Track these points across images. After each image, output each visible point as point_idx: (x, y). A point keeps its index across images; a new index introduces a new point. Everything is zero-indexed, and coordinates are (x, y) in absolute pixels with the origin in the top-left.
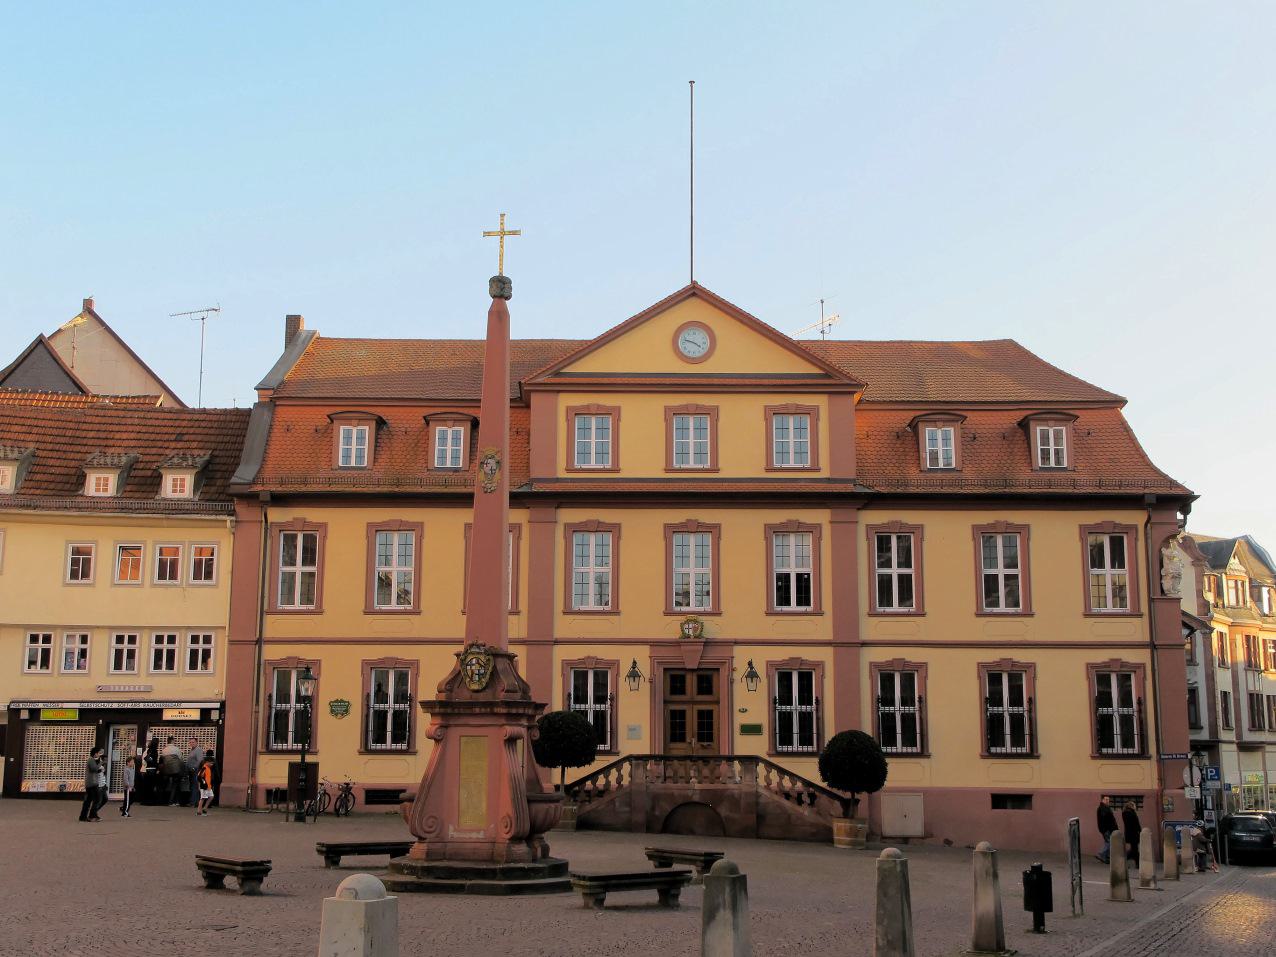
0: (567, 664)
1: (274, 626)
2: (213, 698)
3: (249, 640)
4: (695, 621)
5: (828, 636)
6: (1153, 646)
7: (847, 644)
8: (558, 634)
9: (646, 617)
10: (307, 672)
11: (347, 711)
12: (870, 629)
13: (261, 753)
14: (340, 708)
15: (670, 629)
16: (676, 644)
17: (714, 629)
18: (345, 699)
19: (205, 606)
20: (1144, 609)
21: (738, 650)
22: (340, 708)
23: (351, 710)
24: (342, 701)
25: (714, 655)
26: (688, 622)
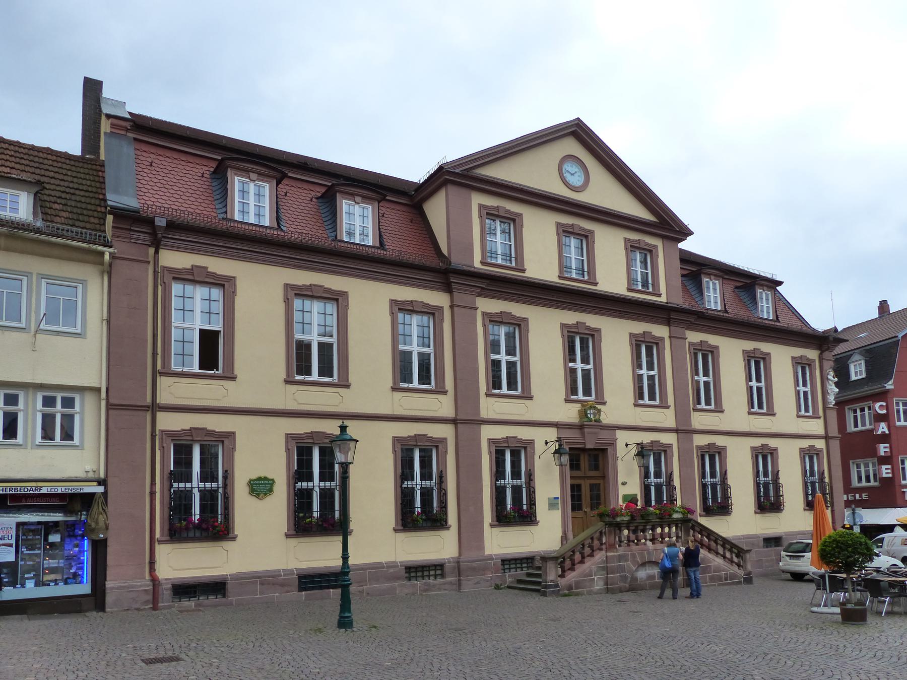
0: (491, 441)
1: (170, 391)
2: (81, 474)
3: (128, 404)
4: (595, 407)
5: (671, 423)
6: (827, 437)
7: (684, 431)
8: (484, 414)
9: (550, 399)
10: (216, 446)
11: (271, 490)
12: (699, 420)
13: (160, 542)
14: (261, 487)
15: (570, 413)
16: (581, 427)
17: (608, 416)
18: (270, 477)
19: (79, 360)
20: (821, 413)
21: (619, 434)
22: (261, 487)
23: (275, 488)
24: (266, 478)
25: (604, 435)
26: (591, 407)
